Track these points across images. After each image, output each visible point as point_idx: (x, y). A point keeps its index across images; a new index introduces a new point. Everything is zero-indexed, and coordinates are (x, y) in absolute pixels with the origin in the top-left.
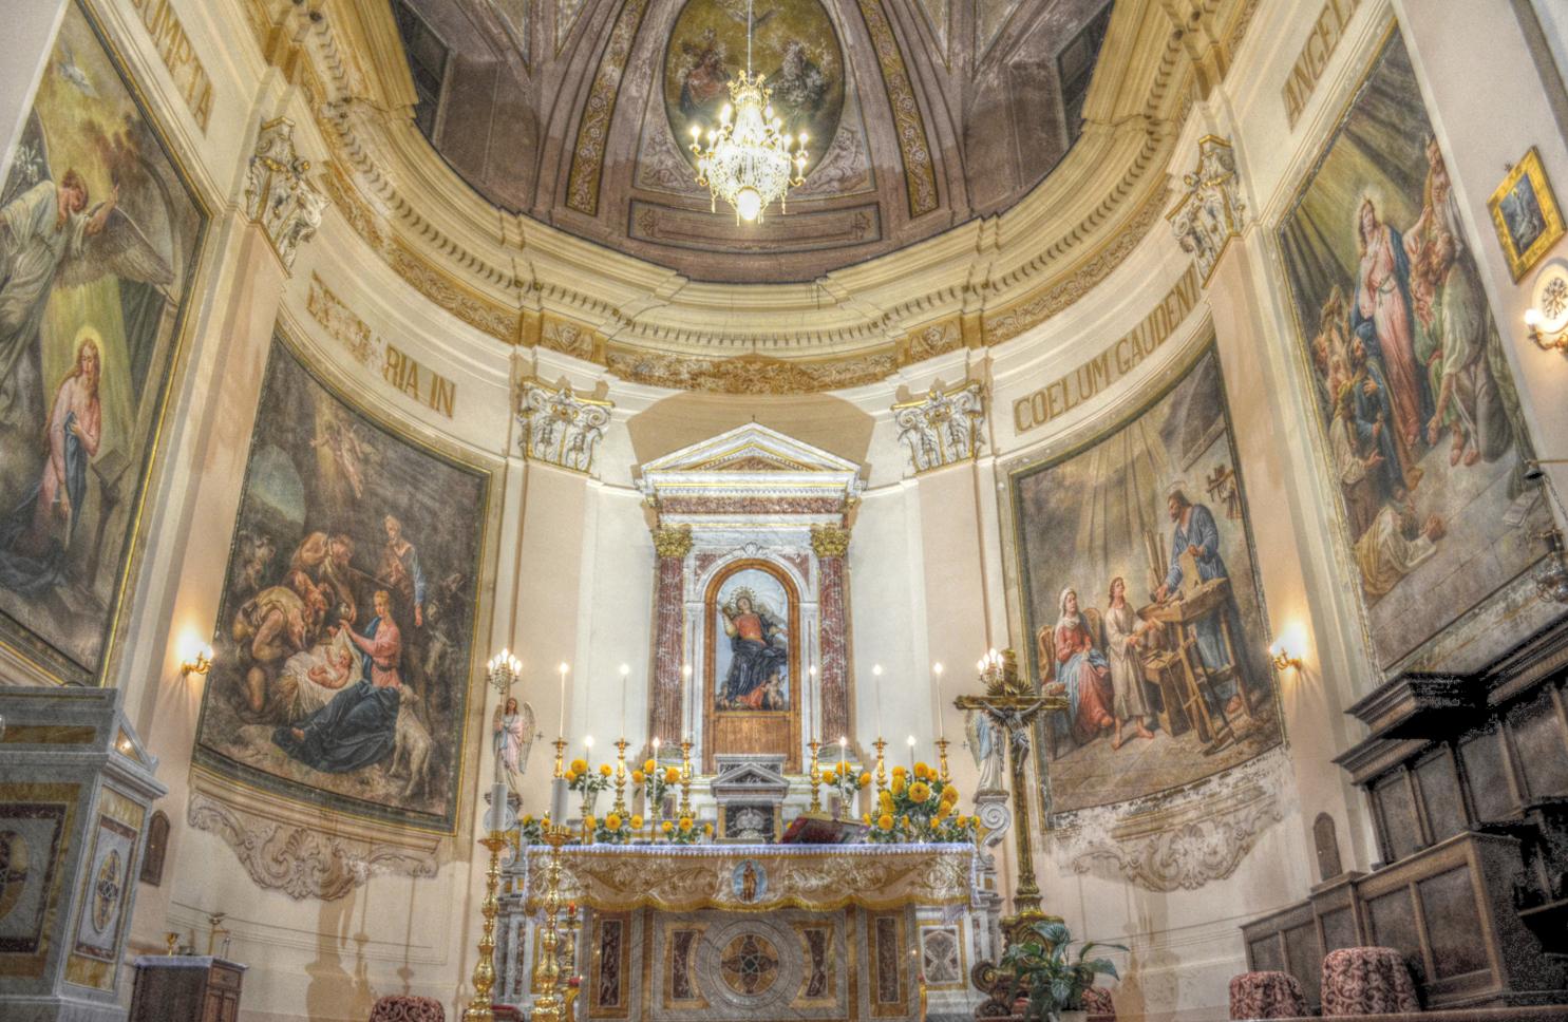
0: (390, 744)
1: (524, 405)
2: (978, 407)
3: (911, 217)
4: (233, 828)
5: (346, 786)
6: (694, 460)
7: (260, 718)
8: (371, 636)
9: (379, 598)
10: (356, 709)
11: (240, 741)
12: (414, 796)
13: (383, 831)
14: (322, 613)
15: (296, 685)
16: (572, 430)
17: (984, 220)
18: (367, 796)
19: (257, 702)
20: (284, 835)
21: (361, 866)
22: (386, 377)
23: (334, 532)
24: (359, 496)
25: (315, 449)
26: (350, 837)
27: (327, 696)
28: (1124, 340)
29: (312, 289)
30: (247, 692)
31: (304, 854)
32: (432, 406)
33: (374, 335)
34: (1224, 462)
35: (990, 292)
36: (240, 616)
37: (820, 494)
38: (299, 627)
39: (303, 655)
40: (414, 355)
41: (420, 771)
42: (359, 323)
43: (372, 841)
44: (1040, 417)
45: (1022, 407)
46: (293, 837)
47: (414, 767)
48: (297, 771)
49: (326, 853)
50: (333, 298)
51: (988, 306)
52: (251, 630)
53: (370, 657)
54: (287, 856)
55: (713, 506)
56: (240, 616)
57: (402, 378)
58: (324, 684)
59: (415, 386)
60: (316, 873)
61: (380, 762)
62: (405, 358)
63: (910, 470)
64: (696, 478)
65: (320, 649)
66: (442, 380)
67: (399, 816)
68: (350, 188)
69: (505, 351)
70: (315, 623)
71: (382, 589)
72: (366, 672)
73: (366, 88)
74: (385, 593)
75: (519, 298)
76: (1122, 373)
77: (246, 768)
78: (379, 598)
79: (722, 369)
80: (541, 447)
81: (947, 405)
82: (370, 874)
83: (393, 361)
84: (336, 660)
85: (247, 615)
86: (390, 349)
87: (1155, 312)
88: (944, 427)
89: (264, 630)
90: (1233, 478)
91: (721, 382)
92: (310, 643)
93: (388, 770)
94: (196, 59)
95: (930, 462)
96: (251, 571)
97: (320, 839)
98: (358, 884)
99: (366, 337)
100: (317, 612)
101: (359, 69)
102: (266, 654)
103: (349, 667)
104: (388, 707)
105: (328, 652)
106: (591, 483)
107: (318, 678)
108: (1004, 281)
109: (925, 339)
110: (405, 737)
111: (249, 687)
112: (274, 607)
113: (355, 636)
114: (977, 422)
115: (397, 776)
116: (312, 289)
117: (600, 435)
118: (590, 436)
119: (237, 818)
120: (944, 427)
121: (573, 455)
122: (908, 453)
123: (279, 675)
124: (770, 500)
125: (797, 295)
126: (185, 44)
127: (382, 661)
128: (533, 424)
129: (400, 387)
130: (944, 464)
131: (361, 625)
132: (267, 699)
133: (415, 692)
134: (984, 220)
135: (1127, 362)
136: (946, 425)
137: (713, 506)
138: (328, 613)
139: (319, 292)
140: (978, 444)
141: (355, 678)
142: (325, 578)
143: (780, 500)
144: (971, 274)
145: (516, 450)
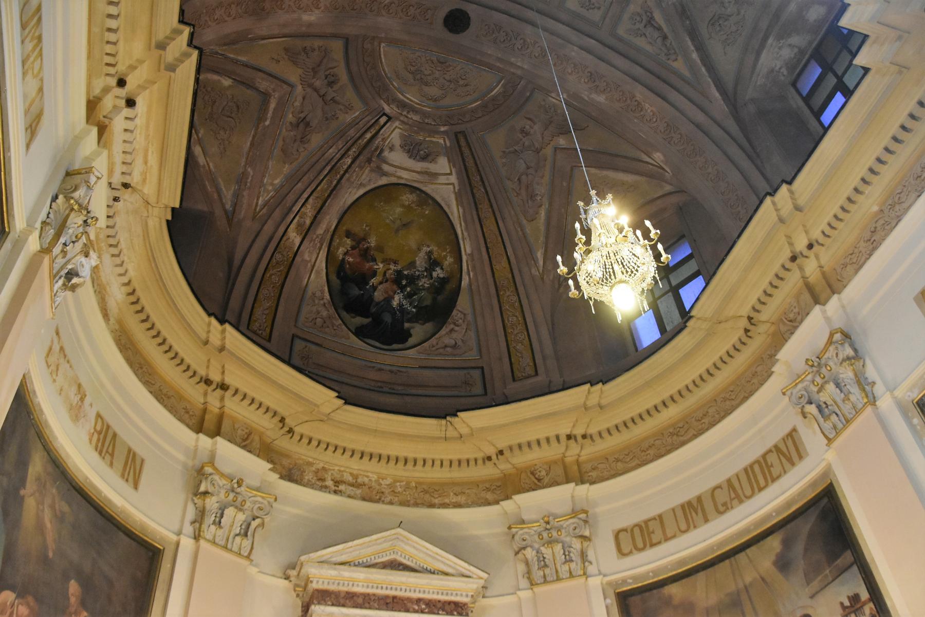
1: (202, 488)
2: (587, 533)
3: (514, 380)
6: (343, 558)
16: (241, 517)
17: (592, 385)
22: (91, 441)
24: (51, 554)
28: (719, 487)
29: (52, 341)
32: (123, 476)
33: (88, 400)
34: (857, 591)
35: (588, 441)
37: (453, 598)
40: (116, 427)
42: (79, 386)
44: (640, 545)
45: (622, 535)
50: (65, 356)
51: (583, 453)
55: (360, 600)
57: (103, 445)
59: (112, 455)
62: (108, 427)
63: (524, 583)
64: (347, 573)
69: (186, 435)
73: (144, 180)
76: (721, 513)
79: (360, 480)
80: (213, 528)
81: (559, 530)
83: (98, 428)
86: (99, 416)
87: (751, 466)
88: (558, 548)
90: (871, 605)
91: (359, 492)
94: (42, 80)
95: (545, 576)
99: (82, 399)
101: (146, 163)
106: (253, 570)
108: (600, 434)
109: (533, 473)
114: (586, 544)
117: (262, 525)
118: (254, 524)
120: (558, 548)
121: (238, 539)
122: (521, 568)
124: (409, 600)
125: (429, 425)
126: (39, 61)
128: (208, 507)
129: (100, 453)
130: (558, 579)
134: (592, 385)
135: (725, 504)
136: (560, 546)
137: (360, 600)
140: (587, 564)
143: (419, 601)
144: (574, 426)
145: (188, 529)
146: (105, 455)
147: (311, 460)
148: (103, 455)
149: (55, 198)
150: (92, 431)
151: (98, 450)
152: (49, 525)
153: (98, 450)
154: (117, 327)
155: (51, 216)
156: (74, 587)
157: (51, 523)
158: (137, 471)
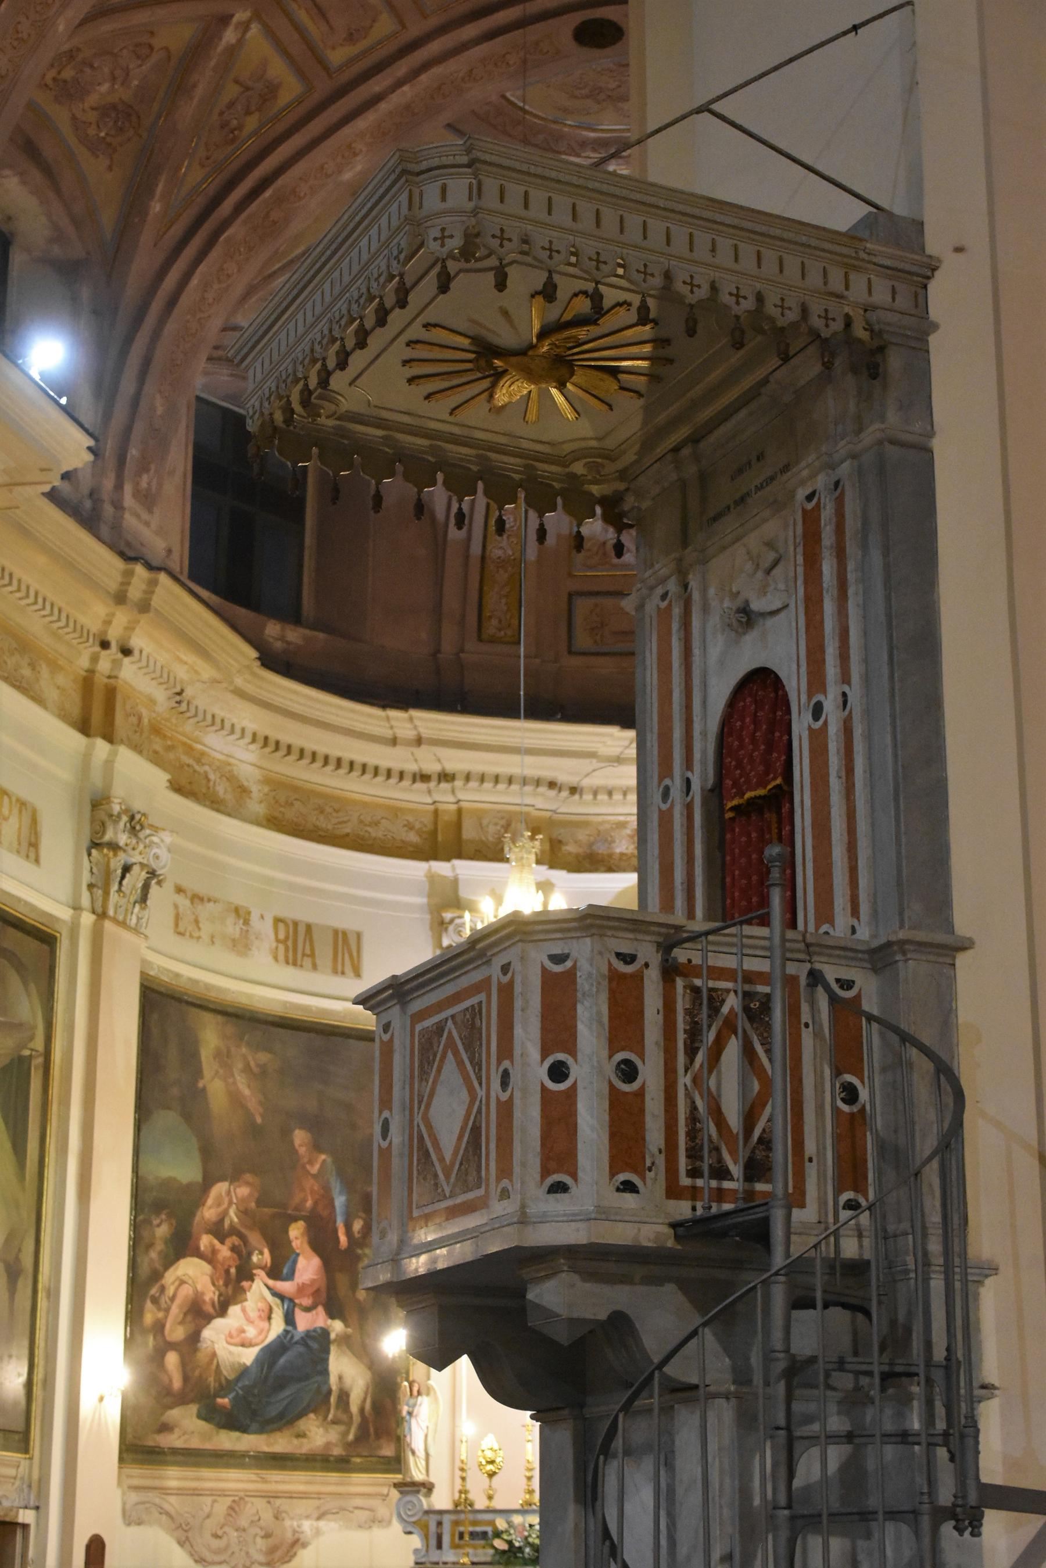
0: (324, 1389)
4: (168, 1514)
5: (280, 1443)
7: (182, 1399)
8: (290, 1276)
9: (296, 1232)
10: (282, 1361)
11: (165, 1428)
12: (358, 1440)
13: (329, 1482)
14: (233, 1270)
15: (214, 1355)
18: (305, 1450)
19: (177, 1383)
20: (221, 1507)
21: (307, 1526)
22: (276, 959)
23: (234, 1177)
24: (259, 1120)
25: (204, 1089)
26: (291, 1496)
27: (248, 1356)
29: (176, 906)
30: (166, 1379)
31: (243, 1522)
32: (335, 972)
36: (149, 1304)
38: (211, 1294)
39: (218, 1322)
40: (304, 916)
41: (362, 1410)
42: (237, 910)
43: (319, 1496)
46: (231, 1508)
47: (354, 1408)
48: (229, 1440)
49: (267, 1516)
50: (202, 899)
52: (161, 1315)
53: (291, 1300)
54: (226, 1529)
56: (149, 1304)
58: (243, 1345)
59: (312, 955)
60: (259, 1540)
61: (315, 1411)
62: (296, 924)
65: (234, 1310)
66: (345, 933)
67: (341, 1464)
68: (203, 754)
69: (416, 870)
70: (226, 1285)
71: (295, 1219)
72: (289, 1319)
74: (301, 1224)
75: (429, 792)
77: (175, 1451)
78: (296, 1232)
82: (318, 1533)
83: (282, 936)
84: (253, 1314)
85: (155, 1301)
86: (277, 921)
89: (175, 1310)
92: (222, 1310)
93: (325, 1418)
94: (18, 800)
96: (153, 1255)
97: (260, 1504)
98: (304, 1545)
99: (246, 922)
100: (227, 1272)
102: (176, 1333)
103: (269, 1318)
104: (321, 1340)
105: (244, 1310)
107: (237, 1340)
110: (340, 1378)
111: (166, 1372)
112: (182, 1282)
113: (271, 1282)
115: (334, 1422)
116: (176, 906)
119: (173, 1503)
123: (196, 1350)
127: (307, 1301)
129: (295, 964)
131: (275, 1272)
132: (186, 1379)
133: (347, 1326)
138: (239, 1269)
139: (184, 902)
141: (277, 1327)
142: (234, 1231)
146: (302, 960)
147: (622, 818)
148: (299, 963)
149: (89, 854)
150: (274, 944)
151: (291, 961)
152: (247, 1092)
153: (291, 961)
154: (266, 789)
155: (95, 870)
156: (300, 1137)
157: (249, 1087)
158: (355, 954)
